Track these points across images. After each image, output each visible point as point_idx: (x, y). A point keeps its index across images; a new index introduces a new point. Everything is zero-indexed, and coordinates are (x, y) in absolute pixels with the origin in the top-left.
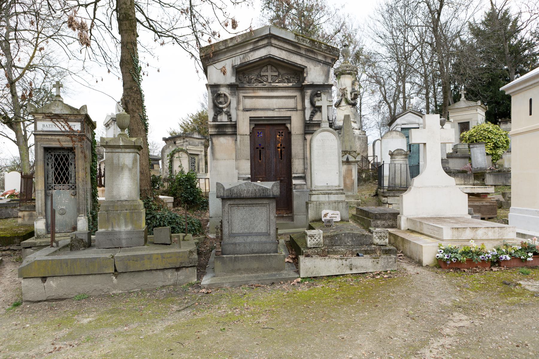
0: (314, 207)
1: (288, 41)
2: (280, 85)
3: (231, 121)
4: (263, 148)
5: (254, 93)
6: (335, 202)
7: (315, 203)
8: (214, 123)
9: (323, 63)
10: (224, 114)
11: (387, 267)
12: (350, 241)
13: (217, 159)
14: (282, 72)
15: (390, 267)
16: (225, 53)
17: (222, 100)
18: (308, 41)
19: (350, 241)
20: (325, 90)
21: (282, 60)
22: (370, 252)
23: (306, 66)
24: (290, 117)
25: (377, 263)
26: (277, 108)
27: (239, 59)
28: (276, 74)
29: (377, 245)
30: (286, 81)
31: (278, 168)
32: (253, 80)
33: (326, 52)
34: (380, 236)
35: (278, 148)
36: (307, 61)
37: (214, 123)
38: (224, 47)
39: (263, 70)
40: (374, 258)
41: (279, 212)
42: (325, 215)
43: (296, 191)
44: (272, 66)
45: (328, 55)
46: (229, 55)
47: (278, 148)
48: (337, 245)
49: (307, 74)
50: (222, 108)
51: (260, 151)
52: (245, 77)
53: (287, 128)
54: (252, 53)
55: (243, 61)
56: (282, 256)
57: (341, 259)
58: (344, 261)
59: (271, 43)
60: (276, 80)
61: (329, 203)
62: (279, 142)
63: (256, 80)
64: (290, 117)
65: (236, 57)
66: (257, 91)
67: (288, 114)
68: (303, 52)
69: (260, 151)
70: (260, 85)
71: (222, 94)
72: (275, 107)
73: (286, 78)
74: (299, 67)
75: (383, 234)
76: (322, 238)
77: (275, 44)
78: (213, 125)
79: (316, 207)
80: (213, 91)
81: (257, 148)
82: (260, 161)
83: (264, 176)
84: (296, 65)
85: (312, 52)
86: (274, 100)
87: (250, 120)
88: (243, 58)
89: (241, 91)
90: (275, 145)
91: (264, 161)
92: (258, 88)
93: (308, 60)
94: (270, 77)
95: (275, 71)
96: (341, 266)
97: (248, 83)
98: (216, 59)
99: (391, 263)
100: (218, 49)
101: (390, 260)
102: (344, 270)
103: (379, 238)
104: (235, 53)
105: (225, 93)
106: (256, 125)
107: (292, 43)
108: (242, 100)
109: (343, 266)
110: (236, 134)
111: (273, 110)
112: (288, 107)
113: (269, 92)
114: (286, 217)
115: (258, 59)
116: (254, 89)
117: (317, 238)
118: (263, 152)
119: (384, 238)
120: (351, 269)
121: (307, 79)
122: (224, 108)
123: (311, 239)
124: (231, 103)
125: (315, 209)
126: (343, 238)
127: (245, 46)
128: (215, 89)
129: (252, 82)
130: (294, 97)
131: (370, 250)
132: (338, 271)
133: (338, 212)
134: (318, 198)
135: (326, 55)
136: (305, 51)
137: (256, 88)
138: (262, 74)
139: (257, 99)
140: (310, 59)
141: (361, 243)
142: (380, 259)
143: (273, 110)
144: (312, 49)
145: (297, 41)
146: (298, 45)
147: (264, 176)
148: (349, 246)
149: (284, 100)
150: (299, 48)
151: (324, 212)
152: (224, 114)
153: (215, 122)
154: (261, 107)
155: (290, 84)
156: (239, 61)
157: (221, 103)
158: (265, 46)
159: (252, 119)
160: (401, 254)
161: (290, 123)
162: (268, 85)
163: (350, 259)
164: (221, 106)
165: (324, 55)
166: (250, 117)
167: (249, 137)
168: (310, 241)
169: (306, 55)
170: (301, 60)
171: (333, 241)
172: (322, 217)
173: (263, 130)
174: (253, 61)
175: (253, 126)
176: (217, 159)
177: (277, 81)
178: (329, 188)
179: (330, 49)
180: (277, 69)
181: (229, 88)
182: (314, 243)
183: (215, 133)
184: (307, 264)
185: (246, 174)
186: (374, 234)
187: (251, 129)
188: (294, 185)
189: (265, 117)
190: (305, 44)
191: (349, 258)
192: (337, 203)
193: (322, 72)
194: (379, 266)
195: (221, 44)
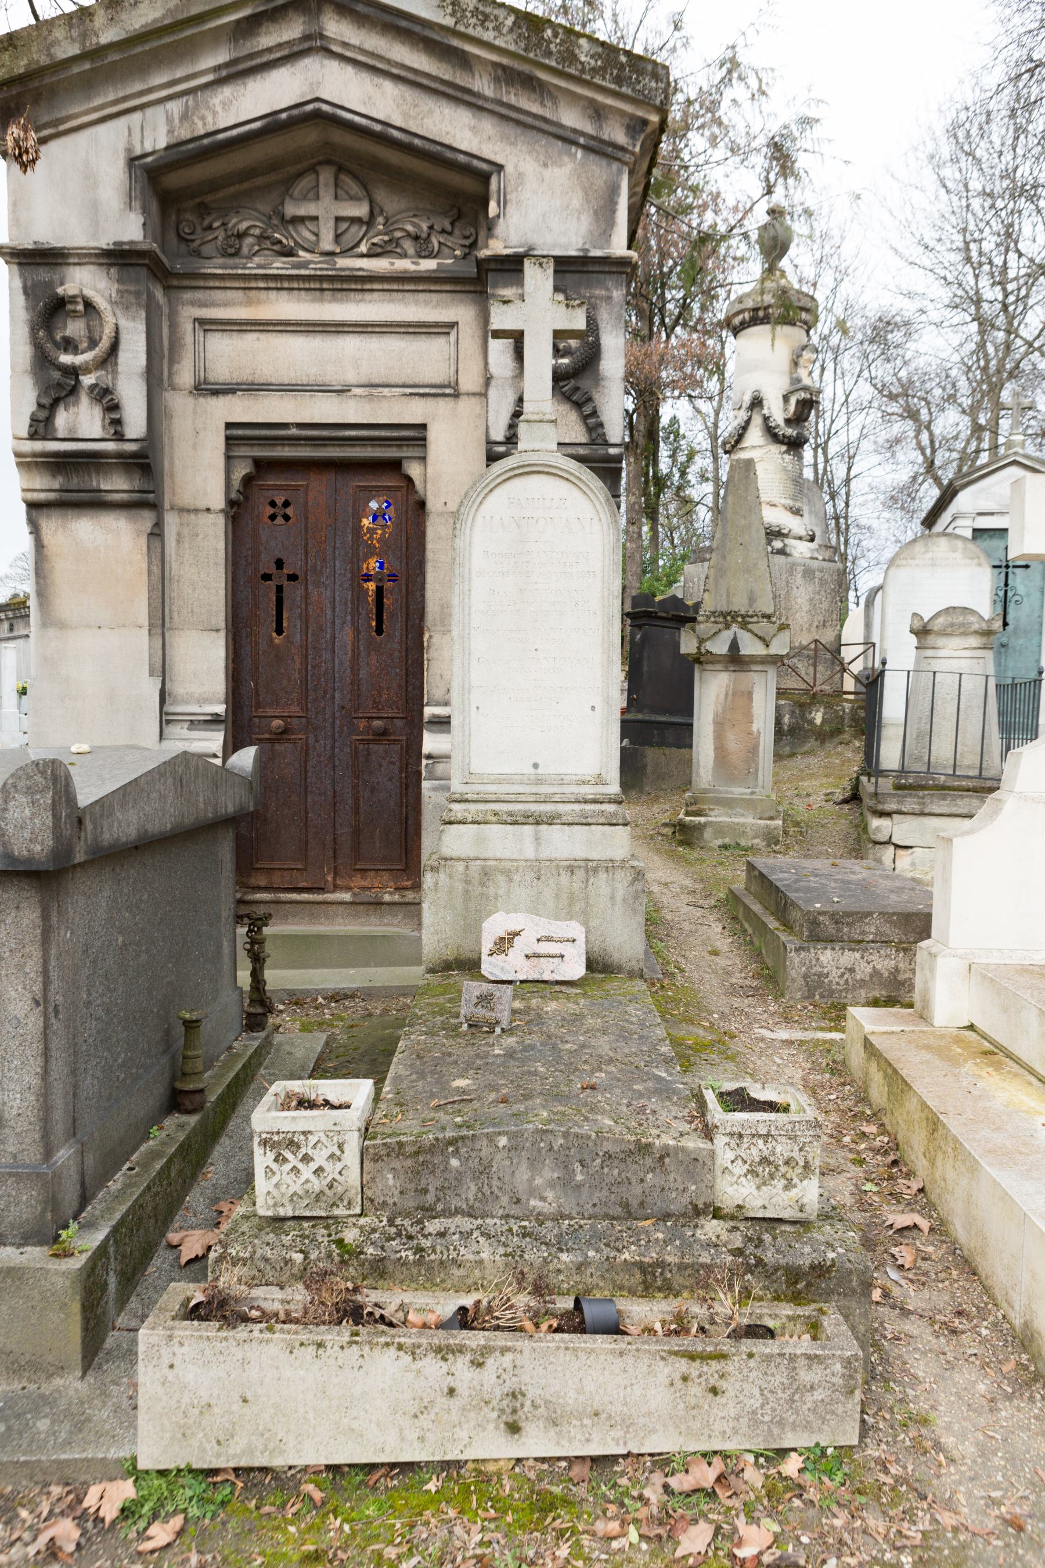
0: (451, 890)
1: (404, 24)
2: (380, 265)
3: (119, 437)
4: (293, 578)
5: (249, 303)
6: (572, 870)
7: (460, 867)
8: (39, 446)
9: (586, 148)
10: (84, 400)
11: (781, 1423)
12: (551, 1184)
13: (62, 626)
14: (391, 203)
15: (807, 1426)
16: (88, 84)
17: (75, 328)
18: (510, 21)
19: (551, 1184)
20: (589, 286)
21: (378, 127)
22: (678, 1280)
23: (499, 160)
24: (423, 427)
25: (714, 1391)
26: (364, 380)
27: (161, 120)
28: (361, 210)
29: (737, 1216)
30: (408, 246)
31: (363, 674)
32: (249, 240)
33: (598, 80)
34: (765, 1161)
35: (368, 578)
36: (505, 138)
37: (39, 446)
38: (74, 50)
39: (296, 192)
40: (692, 1357)
41: (363, 883)
42: (504, 944)
43: (435, 789)
44: (340, 169)
45: (609, 101)
46: (111, 97)
47: (368, 578)
48: (458, 1212)
49: (502, 203)
50: (73, 372)
51: (280, 589)
52: (210, 228)
53: (410, 480)
54: (227, 92)
55: (185, 134)
56: (60, 1281)
57: (438, 1350)
58: (461, 1365)
59: (322, 36)
60: (357, 245)
61: (539, 869)
62: (371, 552)
63: (262, 238)
64: (423, 427)
65: (149, 112)
66: (263, 294)
67: (412, 412)
68: (482, 85)
69: (280, 589)
70: (279, 266)
71: (73, 299)
72: (351, 378)
73: (409, 235)
74: (466, 170)
75: (782, 1149)
76: (352, 1156)
77: (345, 45)
78: (35, 455)
79: (467, 892)
80: (34, 286)
81: (267, 577)
82: (277, 639)
83: (294, 709)
84: (449, 154)
85: (529, 83)
86: (350, 344)
87: (228, 438)
88: (185, 116)
89: (188, 295)
90: (356, 559)
91: (298, 638)
92: (266, 277)
93: (511, 130)
94: (332, 223)
95: (353, 198)
96: (442, 1401)
97: (225, 254)
98: (46, 119)
99: (819, 1395)
100: (44, 60)
101: (806, 1376)
102: (463, 1434)
103: (752, 1172)
104: (138, 87)
105: (89, 293)
106: (258, 462)
107: (428, 33)
108: (189, 339)
109: (455, 1403)
110: (155, 506)
111: (343, 391)
112: (417, 380)
113: (321, 300)
114: (394, 904)
115: (257, 125)
116: (247, 283)
117: (320, 1158)
118: (294, 593)
119: (793, 1174)
120: (514, 1428)
121: (500, 229)
122: (86, 369)
123: (280, 1159)
124: (123, 346)
125: (459, 903)
126: (500, 1163)
127: (188, 49)
128: (43, 274)
129: (245, 250)
130: (446, 328)
131: (682, 1267)
132: (412, 1435)
133: (576, 930)
134: (480, 840)
135: (600, 98)
136: (497, 80)
137: (256, 277)
138: (291, 210)
139: (263, 336)
140: (518, 123)
141: (626, 1206)
142: (730, 1367)
143: (343, 391)
144: (525, 68)
145: (449, 21)
146: (455, 42)
147: (294, 709)
148: (540, 1219)
149: (394, 344)
150: (463, 61)
151: (494, 927)
152: (84, 400)
153: (44, 439)
154: (285, 376)
155: (429, 265)
156: (163, 129)
157: (69, 345)
158: (291, 55)
159: (240, 432)
160: (917, 1219)
161: (423, 459)
162: (316, 265)
163: (509, 1357)
164: (66, 359)
165: (592, 102)
166: (229, 426)
167: (221, 520)
168: (269, 1172)
169: (500, 103)
170: (473, 129)
171: (433, 1184)
172: (485, 951)
173: (296, 488)
174: (234, 132)
175: (242, 470)
176: (62, 626)
177: (363, 248)
178: (544, 789)
179: (621, 68)
180: (365, 187)
181: (113, 271)
182: (297, 1188)
183: (52, 496)
184: (189, 1373)
185: (207, 701)
186: (720, 1140)
187: (236, 484)
188: (429, 757)
189: (300, 426)
190: (489, 36)
191: (504, 1350)
192: (580, 874)
193: (580, 194)
194: (726, 1407)
195: (59, 33)
